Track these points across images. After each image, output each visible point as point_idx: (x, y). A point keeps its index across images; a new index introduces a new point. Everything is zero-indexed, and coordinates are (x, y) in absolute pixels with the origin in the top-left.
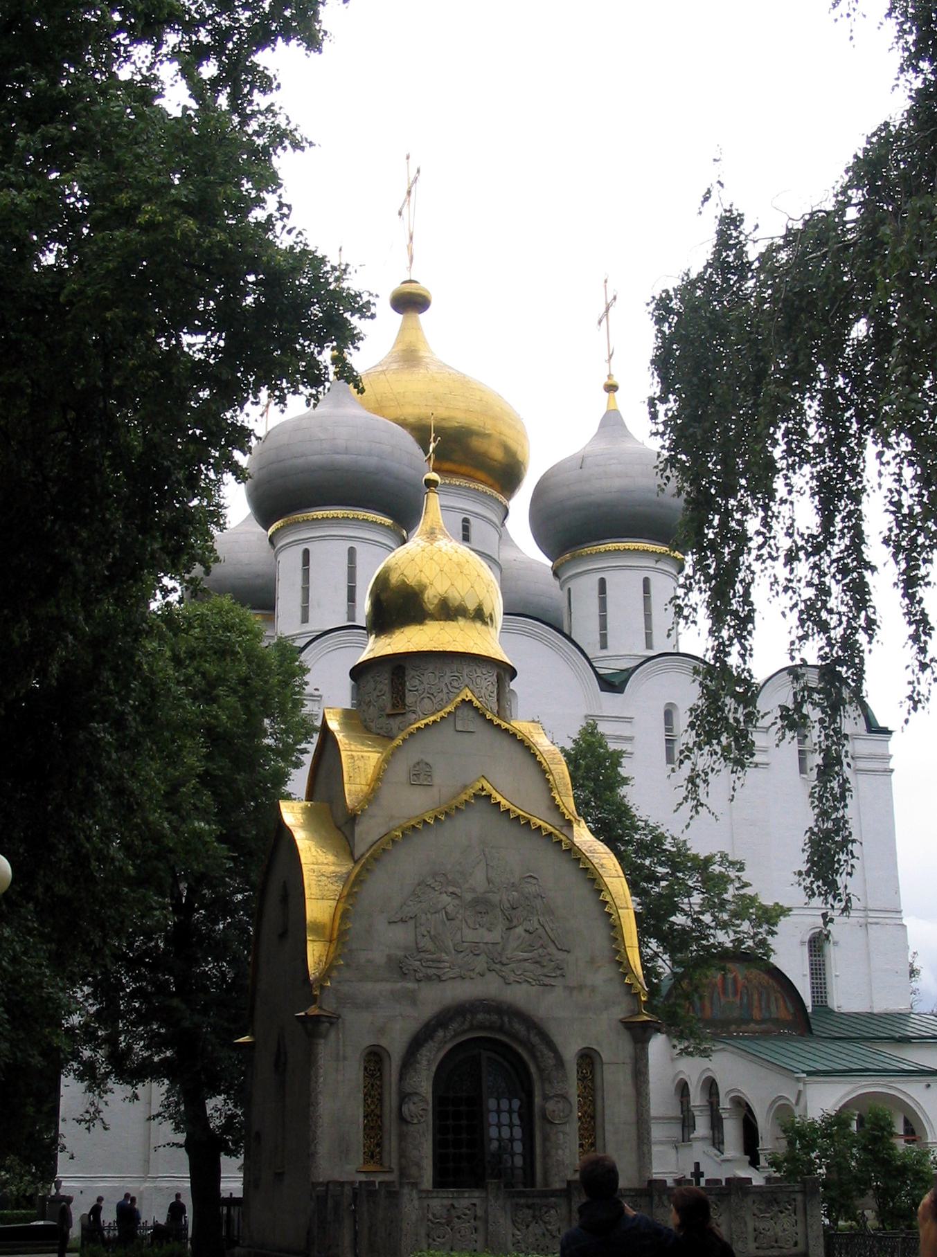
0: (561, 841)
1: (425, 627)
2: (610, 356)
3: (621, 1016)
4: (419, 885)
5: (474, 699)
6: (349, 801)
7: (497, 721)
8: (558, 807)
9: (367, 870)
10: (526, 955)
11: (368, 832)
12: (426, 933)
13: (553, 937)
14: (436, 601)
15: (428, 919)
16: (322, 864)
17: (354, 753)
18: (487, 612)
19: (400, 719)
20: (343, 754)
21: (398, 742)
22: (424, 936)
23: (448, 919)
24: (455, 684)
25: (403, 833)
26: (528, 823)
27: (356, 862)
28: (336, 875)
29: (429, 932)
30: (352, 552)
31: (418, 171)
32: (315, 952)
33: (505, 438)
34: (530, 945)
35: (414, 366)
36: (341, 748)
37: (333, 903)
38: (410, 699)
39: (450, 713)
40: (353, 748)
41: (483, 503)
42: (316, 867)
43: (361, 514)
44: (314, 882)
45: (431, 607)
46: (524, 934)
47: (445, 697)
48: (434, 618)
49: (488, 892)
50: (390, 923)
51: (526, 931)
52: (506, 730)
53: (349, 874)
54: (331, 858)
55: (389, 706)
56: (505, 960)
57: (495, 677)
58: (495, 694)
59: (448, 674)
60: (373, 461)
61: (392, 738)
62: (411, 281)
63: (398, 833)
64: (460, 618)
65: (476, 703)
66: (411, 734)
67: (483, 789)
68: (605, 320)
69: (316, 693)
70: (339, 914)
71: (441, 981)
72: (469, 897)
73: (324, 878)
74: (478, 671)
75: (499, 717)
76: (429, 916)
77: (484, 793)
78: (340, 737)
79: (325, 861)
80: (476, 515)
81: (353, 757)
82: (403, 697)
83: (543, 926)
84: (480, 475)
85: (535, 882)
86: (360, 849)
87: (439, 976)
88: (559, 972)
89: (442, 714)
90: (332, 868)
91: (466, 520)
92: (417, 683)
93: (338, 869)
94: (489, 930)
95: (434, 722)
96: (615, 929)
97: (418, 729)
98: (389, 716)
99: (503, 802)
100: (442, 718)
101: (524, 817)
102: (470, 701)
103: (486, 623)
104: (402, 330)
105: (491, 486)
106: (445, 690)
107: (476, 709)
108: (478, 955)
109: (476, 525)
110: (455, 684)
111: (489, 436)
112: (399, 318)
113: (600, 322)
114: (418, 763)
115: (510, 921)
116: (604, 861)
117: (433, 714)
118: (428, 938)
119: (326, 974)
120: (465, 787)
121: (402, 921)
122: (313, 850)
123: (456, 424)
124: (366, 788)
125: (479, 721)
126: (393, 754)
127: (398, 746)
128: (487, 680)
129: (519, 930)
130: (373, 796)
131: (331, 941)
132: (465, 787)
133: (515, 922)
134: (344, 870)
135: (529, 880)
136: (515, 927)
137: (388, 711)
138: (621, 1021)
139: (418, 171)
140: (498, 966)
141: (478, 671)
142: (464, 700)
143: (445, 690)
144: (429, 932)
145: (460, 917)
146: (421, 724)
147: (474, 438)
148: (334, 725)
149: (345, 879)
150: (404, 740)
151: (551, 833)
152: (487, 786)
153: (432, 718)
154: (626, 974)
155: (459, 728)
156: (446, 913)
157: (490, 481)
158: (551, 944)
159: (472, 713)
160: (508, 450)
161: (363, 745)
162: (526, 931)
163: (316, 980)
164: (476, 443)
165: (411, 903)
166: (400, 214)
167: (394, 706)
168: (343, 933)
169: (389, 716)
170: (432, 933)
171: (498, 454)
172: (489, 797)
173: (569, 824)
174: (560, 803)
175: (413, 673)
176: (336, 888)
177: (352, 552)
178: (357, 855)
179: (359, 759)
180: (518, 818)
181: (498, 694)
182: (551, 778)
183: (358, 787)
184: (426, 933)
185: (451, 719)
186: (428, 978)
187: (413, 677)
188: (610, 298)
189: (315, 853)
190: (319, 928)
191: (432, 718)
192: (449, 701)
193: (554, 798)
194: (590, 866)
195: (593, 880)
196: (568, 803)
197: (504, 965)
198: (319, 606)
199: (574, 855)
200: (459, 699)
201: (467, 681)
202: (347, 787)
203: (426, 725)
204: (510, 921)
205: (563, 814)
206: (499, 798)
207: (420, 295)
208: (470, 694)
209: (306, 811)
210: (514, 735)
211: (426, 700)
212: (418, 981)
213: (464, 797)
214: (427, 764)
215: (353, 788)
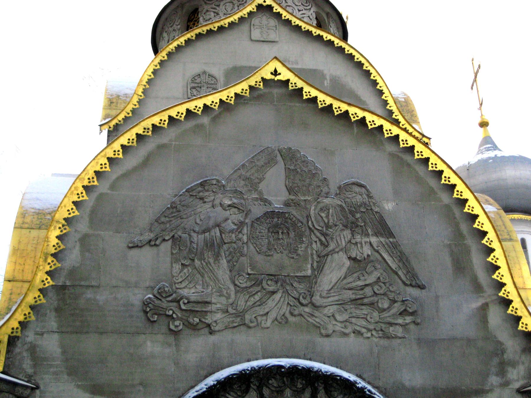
5: (274, 4)
56: (317, 299)
67: (275, 73)
71: (211, 333)
72: (258, 211)
83: (378, 252)
92: (212, 14)
102: (270, 7)
125: (284, 30)
133: (332, 246)
135: (357, 189)
136: (333, 252)
159: (273, 22)
175: (206, 7)
185: (245, 27)
187: (207, 11)
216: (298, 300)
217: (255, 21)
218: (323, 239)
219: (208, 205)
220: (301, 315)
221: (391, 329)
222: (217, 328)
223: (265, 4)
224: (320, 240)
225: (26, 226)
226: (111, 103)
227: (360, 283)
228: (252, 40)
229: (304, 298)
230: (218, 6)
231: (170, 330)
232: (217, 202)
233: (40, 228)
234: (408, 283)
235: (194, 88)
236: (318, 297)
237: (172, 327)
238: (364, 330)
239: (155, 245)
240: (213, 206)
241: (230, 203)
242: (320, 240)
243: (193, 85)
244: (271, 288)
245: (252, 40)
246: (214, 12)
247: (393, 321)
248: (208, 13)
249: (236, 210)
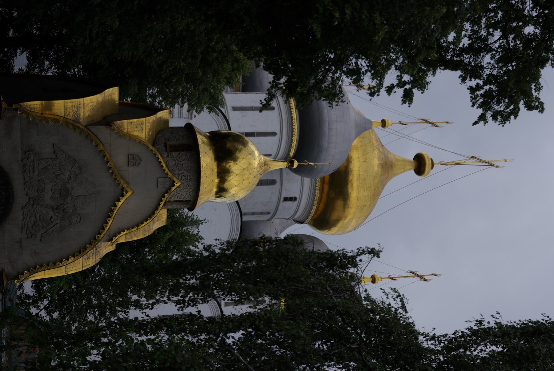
0: (100, 234)
1: (213, 161)
2: (392, 279)
3: (6, 270)
4: (74, 159)
6: (118, 123)
7: (164, 200)
8: (119, 233)
9: (81, 132)
10: (38, 217)
11: (103, 132)
12: (48, 164)
13: (48, 231)
14: (227, 166)
15: (56, 164)
16: (84, 109)
17: (144, 125)
18: (223, 194)
19: (164, 149)
20: (144, 119)
21: (151, 147)
22: (47, 162)
23: (56, 175)
24: (183, 178)
25: (101, 150)
26: (110, 217)
27: (86, 127)
28: (77, 116)
29: (49, 165)
30: (273, 134)
31: (497, 167)
32: (36, 105)
33: (343, 219)
34: (44, 219)
35: (383, 166)
36: (147, 118)
37: (63, 115)
38: (175, 154)
39: (167, 174)
40: (148, 124)
41: (305, 209)
42: (82, 105)
43: (295, 138)
44: (74, 104)
45: (224, 164)
46: (50, 216)
47: (176, 172)
48: (219, 166)
49: (72, 196)
50: (53, 144)
51: (52, 217)
52: (159, 205)
53: (79, 123)
54: (87, 114)
55: (171, 143)
57: (188, 199)
58: (179, 199)
59: (189, 174)
60: (325, 143)
61: (153, 145)
62: (433, 165)
63: (101, 148)
64: (219, 179)
65: (173, 188)
66: (155, 154)
67: (127, 192)
68: (413, 275)
69: (193, 116)
70: (58, 118)
71: (23, 172)
72: (69, 186)
73: (76, 109)
74: (191, 190)
75: (166, 202)
76: (57, 165)
77: (124, 193)
78: (152, 118)
79: (85, 111)
80: (299, 205)
81: (142, 124)
82: (175, 150)
83: (54, 226)
84: (322, 206)
85: (78, 221)
86: (93, 129)
87: (25, 171)
88: (29, 235)
89: (167, 170)
90: (82, 114)
91: (295, 199)
92: (183, 158)
93: (81, 117)
94: (51, 197)
95: (162, 167)
96: (54, 264)
97: (158, 158)
98: (165, 143)
99: (120, 203)
100: (164, 170)
101: (112, 215)
102: (174, 185)
103: (217, 193)
104: (405, 161)
105: (316, 212)
106: (180, 172)
107: (170, 189)
108: (37, 192)
109: (293, 205)
110: (183, 178)
111: (344, 211)
112: (411, 158)
113: (411, 272)
114: (140, 159)
115: (56, 209)
116: (91, 259)
117: (167, 166)
118: (46, 165)
119: (24, 111)
120: (128, 183)
121: (54, 152)
122: (91, 104)
123: (350, 192)
124: (125, 131)
126: (144, 145)
127: (148, 148)
128: (186, 195)
129: (52, 214)
130: (121, 135)
131: (42, 113)
132: (128, 183)
133: (56, 211)
134: (81, 120)
135: (79, 219)
136: (53, 211)
137: (168, 143)
138: (3, 270)
139: (497, 167)
140: (32, 203)
141: (191, 190)
142: (174, 182)
143: (180, 172)
144: (49, 165)
145: (57, 182)
146: (161, 159)
147: (342, 202)
148: (160, 114)
149: (76, 120)
150: (152, 151)
151: (104, 229)
152: (129, 194)
153: (164, 165)
154: (29, 271)
155: (159, 179)
156: (60, 174)
157: (318, 213)
158: (44, 231)
159: (167, 186)
160: (337, 221)
161: (150, 130)
162: (52, 217)
163: (21, 106)
164: (339, 203)
165: (64, 156)
166: (473, 157)
167: (171, 146)
168: (47, 119)
169: (165, 143)
170: (49, 167)
171: (334, 217)
172: (123, 196)
173: (110, 240)
174: (121, 235)
176: (71, 116)
177: (273, 134)
178: (90, 127)
179: (141, 127)
180: (112, 211)
181: (179, 201)
182: (135, 229)
183: (126, 127)
184: (48, 164)
186: (24, 166)
187: (186, 155)
188: (426, 278)
189: (90, 105)
190: (49, 108)
191: (164, 165)
192: (174, 175)
193: (124, 231)
194: (87, 251)
195: (80, 252)
196: (122, 239)
197: (33, 205)
198: (243, 116)
199: (93, 242)
200: (175, 179)
201: (185, 184)
202: (126, 121)
203: (160, 162)
204: (56, 209)
205: (115, 236)
206: (122, 201)
207: (425, 169)
208: (177, 185)
209: (113, 100)
210: (157, 209)
211: (174, 163)
212: (22, 160)
213: (122, 182)
214: (140, 163)
215: (126, 125)
216: (35, 200)
217: (167, 179)
218: (58, 208)
219: (70, 169)
220: (29, 200)
221: (25, 230)
222: (24, 174)
223: (175, 183)
224: (58, 207)
225: (66, 104)
226: (131, 123)
227: (42, 220)
228: (158, 178)
229: (36, 202)
230: (188, 160)
231: (23, 159)
232: (72, 173)
233: (65, 109)
234: (43, 236)
235: (134, 157)
236: (36, 206)
237: (24, 160)
238: (25, 220)
239: (54, 153)
240: (70, 171)
241: (72, 177)
242: (58, 207)
243: (135, 157)
244: (39, 191)
245: (158, 178)
246: (185, 159)
247: (28, 230)
248: (185, 156)
249: (69, 179)
